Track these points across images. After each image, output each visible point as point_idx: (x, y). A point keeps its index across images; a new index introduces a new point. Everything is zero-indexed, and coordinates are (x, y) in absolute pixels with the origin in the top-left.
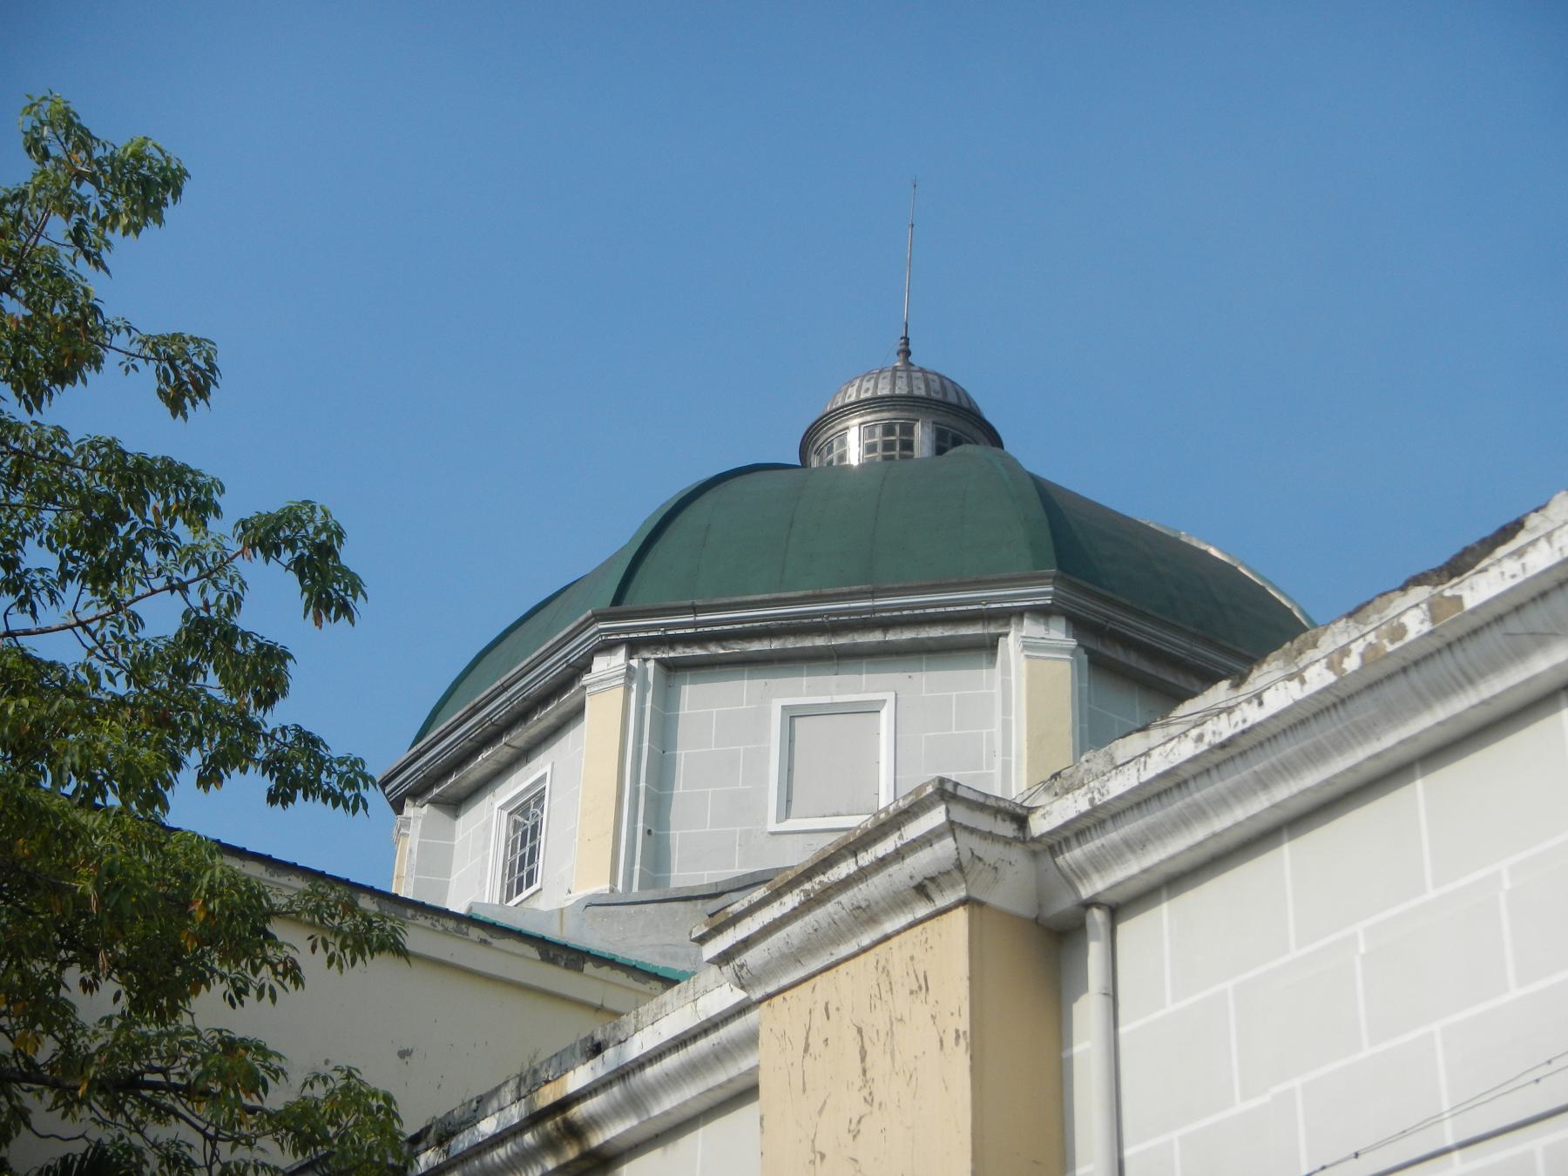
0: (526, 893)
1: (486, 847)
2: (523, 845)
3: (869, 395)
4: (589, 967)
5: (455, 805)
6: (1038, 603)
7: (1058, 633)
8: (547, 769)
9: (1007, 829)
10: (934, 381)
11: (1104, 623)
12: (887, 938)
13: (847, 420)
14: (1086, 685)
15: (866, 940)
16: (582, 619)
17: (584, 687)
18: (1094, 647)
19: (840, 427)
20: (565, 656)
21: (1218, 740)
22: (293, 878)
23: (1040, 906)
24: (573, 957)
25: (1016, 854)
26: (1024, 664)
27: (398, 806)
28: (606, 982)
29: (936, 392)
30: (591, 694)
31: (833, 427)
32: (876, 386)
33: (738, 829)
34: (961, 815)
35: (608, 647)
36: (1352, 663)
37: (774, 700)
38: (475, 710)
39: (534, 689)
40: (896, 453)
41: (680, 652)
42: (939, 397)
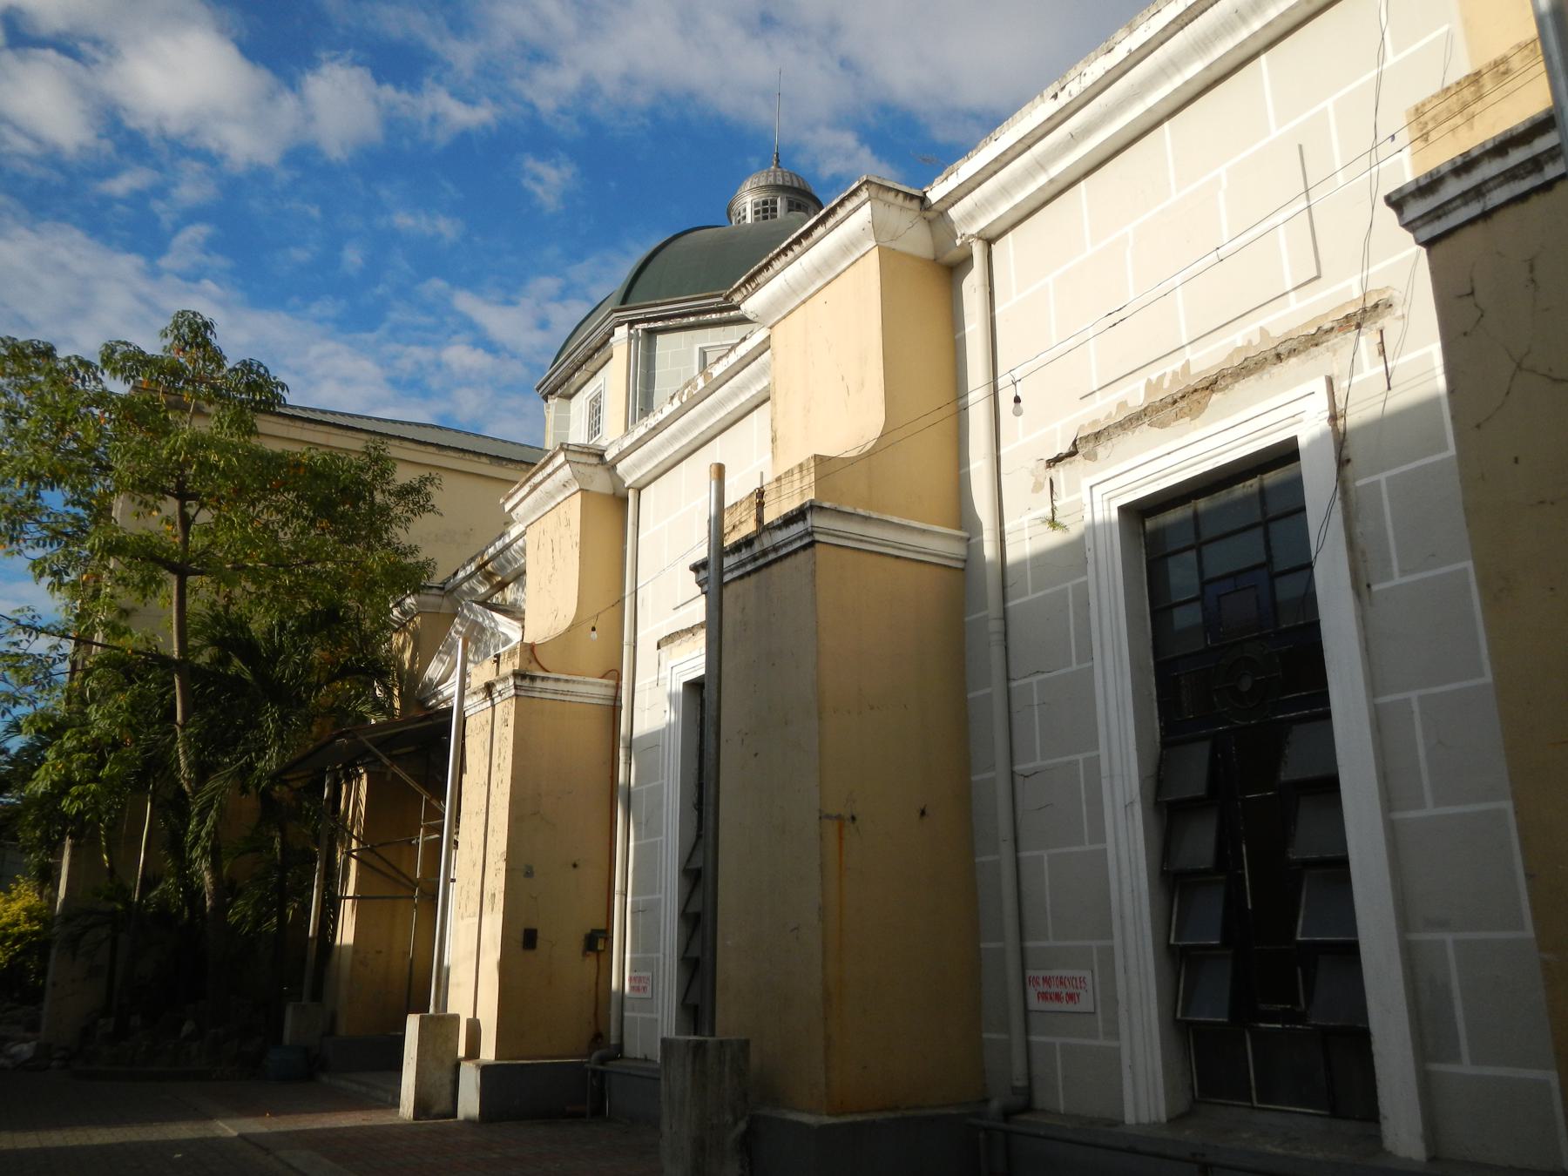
0: (598, 436)
1: (581, 417)
3: (755, 186)
5: (570, 397)
9: (595, 460)
12: (559, 504)
15: (553, 505)
17: (612, 344)
21: (651, 427)
23: (614, 489)
25: (600, 469)
34: (572, 457)
35: (621, 324)
36: (684, 399)
38: (570, 355)
39: (593, 345)
41: (652, 325)
42: (789, 184)
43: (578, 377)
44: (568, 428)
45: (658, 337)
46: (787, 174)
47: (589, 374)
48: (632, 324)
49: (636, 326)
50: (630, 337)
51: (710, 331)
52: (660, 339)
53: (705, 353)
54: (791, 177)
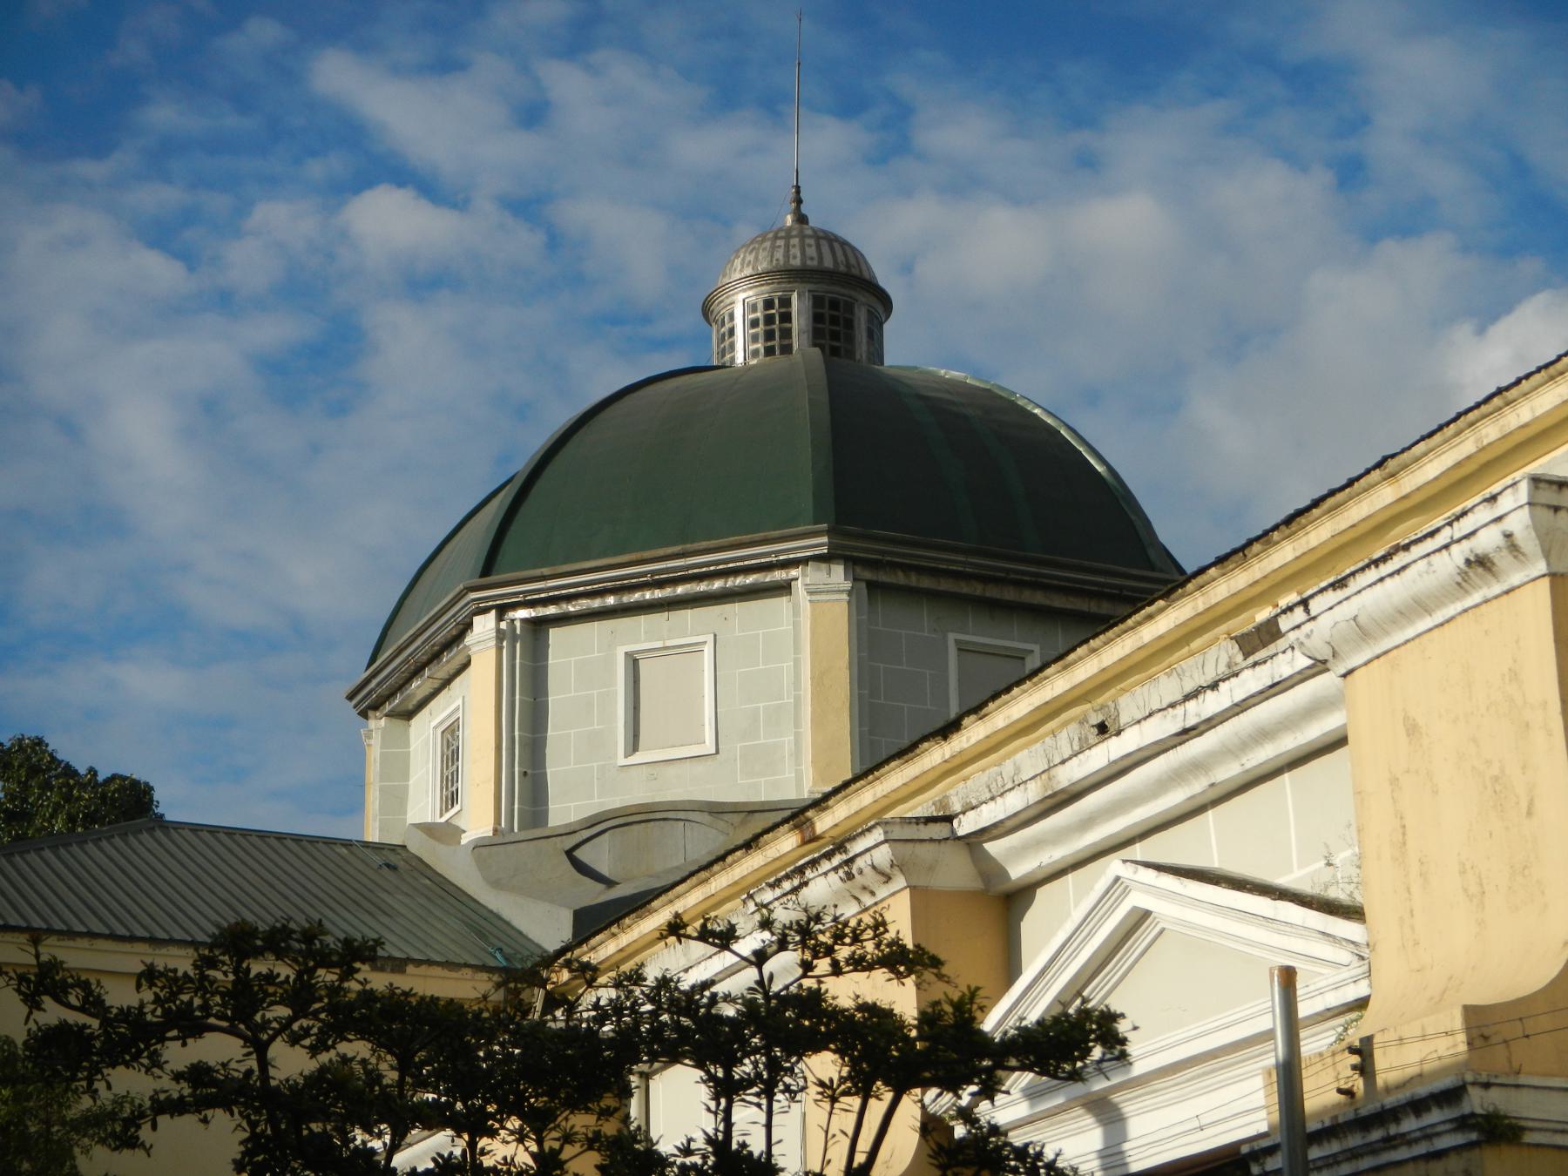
1: (428, 762)
2: (453, 764)
4: (410, 969)
5: (409, 715)
6: (816, 553)
7: (837, 575)
8: (459, 702)
10: (810, 246)
11: (880, 557)
13: (733, 295)
14: (865, 617)
16: (457, 590)
18: (875, 578)
19: (728, 301)
20: (454, 616)
22: (170, 948)
24: (398, 963)
26: (808, 604)
27: (364, 714)
28: (425, 976)
29: (812, 259)
30: (475, 653)
31: (721, 302)
32: (756, 258)
33: (595, 764)
35: (485, 611)
37: (618, 648)
38: (400, 651)
39: (439, 638)
40: (776, 327)
42: (813, 264)
43: (418, 687)
44: (405, 774)
45: (551, 630)
46: (812, 241)
47: (437, 684)
48: (502, 611)
49: (511, 615)
50: (500, 636)
51: (643, 621)
52: (555, 634)
53: (636, 661)
54: (818, 247)
